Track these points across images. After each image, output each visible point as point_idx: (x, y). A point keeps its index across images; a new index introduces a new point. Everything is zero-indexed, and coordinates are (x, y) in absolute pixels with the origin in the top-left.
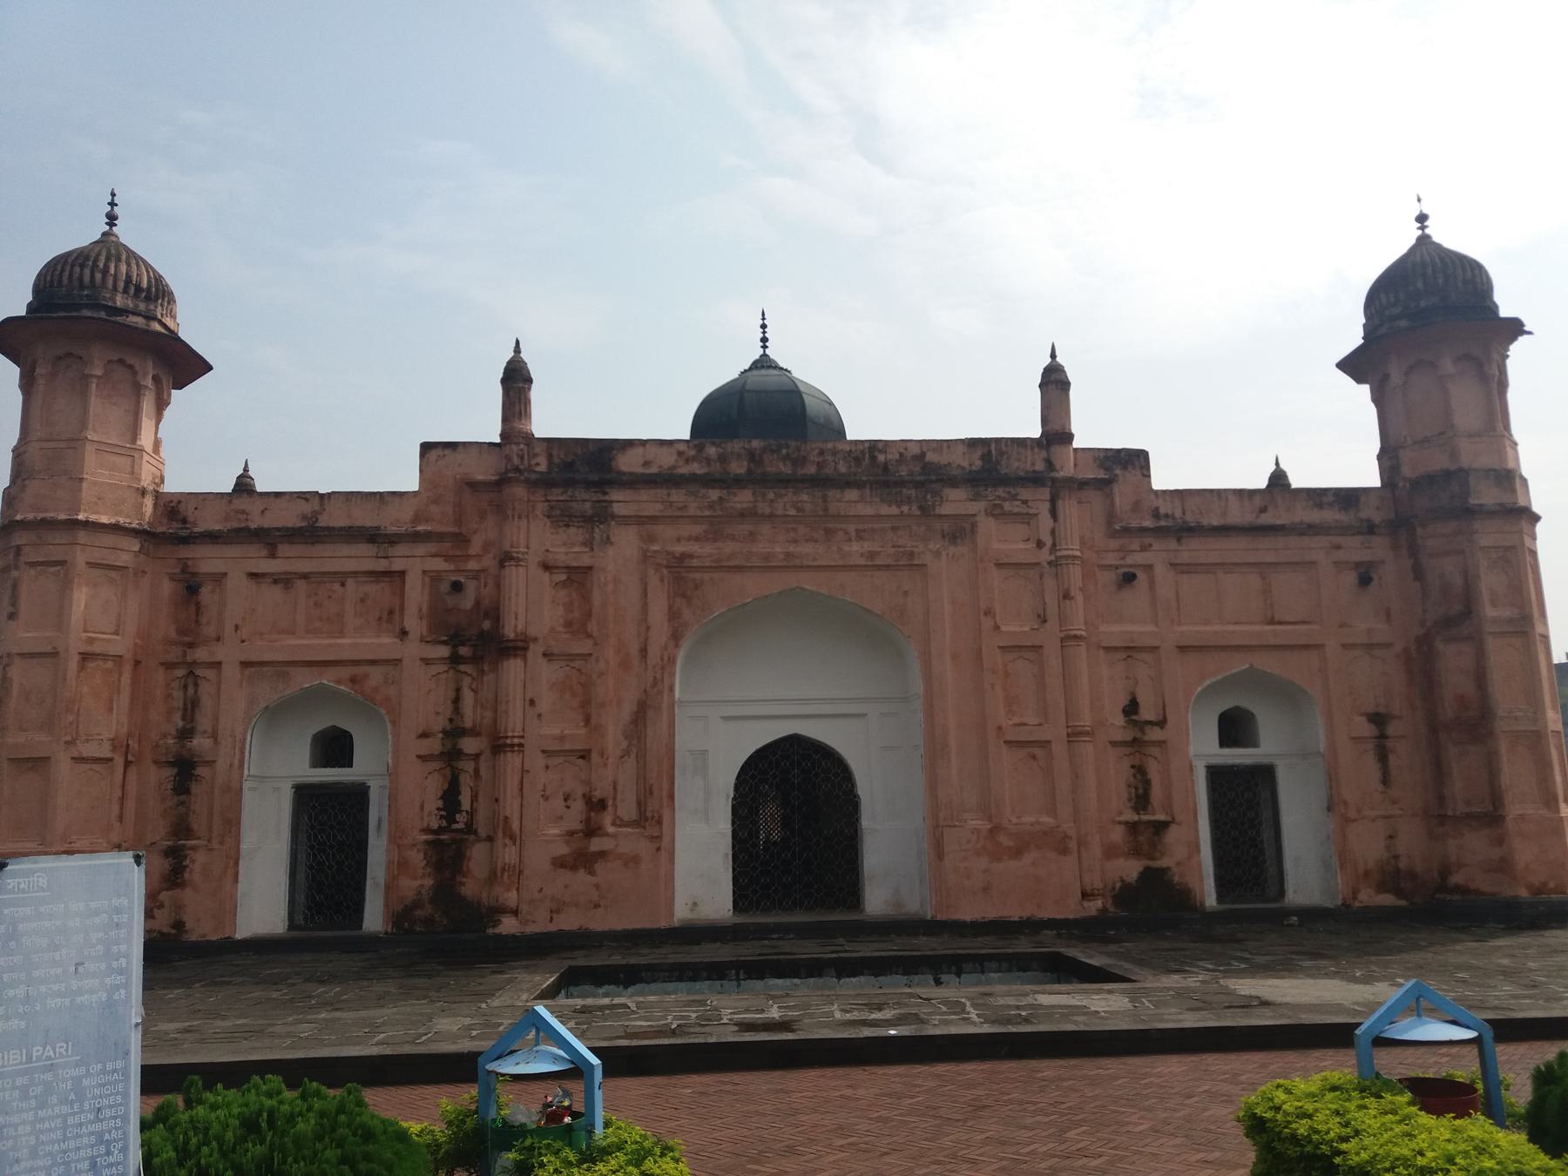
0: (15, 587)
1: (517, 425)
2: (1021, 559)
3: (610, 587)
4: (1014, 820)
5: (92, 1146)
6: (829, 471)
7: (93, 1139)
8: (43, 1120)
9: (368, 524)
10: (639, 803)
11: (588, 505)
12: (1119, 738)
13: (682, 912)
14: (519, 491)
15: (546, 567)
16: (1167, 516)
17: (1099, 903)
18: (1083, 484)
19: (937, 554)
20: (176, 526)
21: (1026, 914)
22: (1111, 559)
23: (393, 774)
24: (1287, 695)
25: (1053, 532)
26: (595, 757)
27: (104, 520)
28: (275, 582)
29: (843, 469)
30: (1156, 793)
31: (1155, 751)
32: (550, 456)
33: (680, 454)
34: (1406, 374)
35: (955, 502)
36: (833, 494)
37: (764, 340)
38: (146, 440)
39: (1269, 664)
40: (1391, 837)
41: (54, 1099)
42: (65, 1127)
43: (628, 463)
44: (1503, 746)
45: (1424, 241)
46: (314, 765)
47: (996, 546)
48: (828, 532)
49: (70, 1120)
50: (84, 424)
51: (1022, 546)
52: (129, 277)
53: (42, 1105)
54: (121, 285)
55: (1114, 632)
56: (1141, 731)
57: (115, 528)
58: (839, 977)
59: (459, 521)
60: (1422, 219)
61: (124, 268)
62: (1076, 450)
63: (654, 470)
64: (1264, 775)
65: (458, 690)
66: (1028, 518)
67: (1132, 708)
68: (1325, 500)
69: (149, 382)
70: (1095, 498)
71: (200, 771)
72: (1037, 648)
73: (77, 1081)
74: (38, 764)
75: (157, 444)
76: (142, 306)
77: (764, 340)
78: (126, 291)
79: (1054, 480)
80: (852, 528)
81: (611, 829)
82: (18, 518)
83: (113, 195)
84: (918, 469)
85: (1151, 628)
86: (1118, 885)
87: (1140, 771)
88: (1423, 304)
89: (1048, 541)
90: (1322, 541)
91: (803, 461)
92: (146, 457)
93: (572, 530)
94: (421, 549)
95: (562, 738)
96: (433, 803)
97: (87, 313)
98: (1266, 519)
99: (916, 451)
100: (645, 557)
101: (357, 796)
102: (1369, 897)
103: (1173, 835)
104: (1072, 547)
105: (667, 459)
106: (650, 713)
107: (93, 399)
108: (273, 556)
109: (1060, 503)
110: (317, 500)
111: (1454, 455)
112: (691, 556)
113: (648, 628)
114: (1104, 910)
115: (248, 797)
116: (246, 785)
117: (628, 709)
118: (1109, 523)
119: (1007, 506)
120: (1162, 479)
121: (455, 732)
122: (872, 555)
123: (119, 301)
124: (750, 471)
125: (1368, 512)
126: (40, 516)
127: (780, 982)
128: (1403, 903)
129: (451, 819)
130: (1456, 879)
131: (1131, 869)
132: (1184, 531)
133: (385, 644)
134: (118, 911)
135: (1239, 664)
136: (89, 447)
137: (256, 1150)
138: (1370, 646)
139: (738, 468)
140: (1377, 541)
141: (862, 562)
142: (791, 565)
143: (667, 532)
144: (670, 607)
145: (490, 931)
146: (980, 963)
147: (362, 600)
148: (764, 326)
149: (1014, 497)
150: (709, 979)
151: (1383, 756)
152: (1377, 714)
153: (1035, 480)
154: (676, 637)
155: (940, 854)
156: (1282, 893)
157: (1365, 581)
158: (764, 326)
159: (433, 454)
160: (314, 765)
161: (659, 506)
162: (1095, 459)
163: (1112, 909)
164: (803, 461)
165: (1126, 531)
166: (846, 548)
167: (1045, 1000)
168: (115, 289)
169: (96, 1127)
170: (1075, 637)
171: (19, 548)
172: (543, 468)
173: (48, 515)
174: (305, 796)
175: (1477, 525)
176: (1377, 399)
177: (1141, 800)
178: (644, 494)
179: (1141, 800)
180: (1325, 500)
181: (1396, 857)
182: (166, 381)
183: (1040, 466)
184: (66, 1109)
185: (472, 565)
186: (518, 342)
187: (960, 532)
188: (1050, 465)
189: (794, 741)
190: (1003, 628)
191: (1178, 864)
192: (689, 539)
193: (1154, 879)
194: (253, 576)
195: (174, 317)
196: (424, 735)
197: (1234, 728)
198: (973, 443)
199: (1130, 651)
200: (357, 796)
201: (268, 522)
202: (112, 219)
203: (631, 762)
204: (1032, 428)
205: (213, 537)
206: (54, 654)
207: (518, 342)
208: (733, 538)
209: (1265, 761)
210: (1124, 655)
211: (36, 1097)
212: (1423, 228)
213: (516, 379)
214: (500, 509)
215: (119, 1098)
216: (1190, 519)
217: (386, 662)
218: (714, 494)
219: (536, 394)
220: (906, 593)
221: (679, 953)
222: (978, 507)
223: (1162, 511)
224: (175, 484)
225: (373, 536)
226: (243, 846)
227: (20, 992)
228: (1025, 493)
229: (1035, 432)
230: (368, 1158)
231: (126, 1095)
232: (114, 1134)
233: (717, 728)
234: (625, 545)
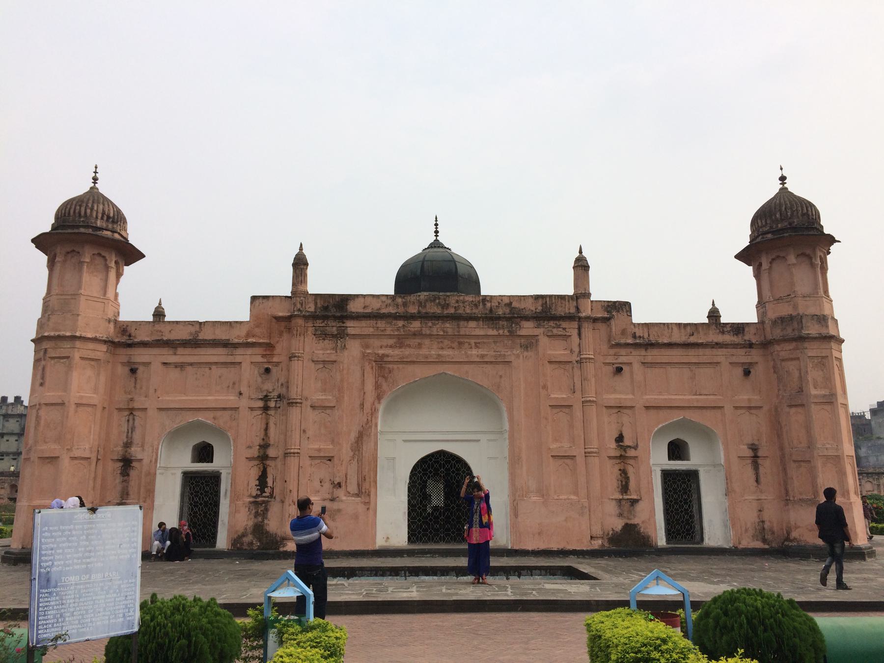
0: (44, 369)
1: (301, 288)
3: (345, 372)
4: (556, 497)
6: (460, 311)
9: (224, 338)
10: (358, 485)
11: (335, 328)
12: (613, 454)
13: (380, 543)
14: (300, 322)
16: (640, 337)
17: (600, 542)
18: (595, 320)
19: (518, 356)
20: (125, 339)
21: (561, 547)
22: (610, 359)
23: (234, 467)
24: (706, 434)
25: (579, 345)
26: (336, 460)
27: (89, 336)
28: (176, 367)
29: (468, 311)
30: (632, 484)
31: (631, 462)
32: (316, 304)
34: (771, 263)
35: (528, 328)
36: (462, 323)
37: (437, 232)
38: (110, 295)
39: (694, 417)
40: (760, 511)
44: (819, 463)
45: (784, 190)
46: (193, 461)
47: (549, 352)
48: (460, 343)
50: (80, 288)
52: (103, 210)
54: (100, 215)
55: (612, 398)
56: (624, 452)
57: (95, 340)
58: (457, 576)
60: (783, 179)
61: (101, 207)
63: (369, 310)
64: (692, 476)
65: (267, 424)
66: (566, 337)
67: (620, 439)
68: (725, 329)
69: (113, 264)
70: (601, 326)
71: (134, 464)
72: (570, 406)
73: (119, 586)
74: (53, 460)
75: (116, 295)
76: (110, 226)
77: (437, 232)
78: (102, 218)
79: (580, 318)
81: (344, 498)
82: (46, 334)
83: (96, 167)
84: (508, 311)
85: (631, 396)
86: (611, 533)
87: (624, 472)
88: (779, 226)
89: (576, 350)
90: (724, 351)
91: (447, 306)
92: (111, 303)
93: (326, 342)
94: (250, 351)
95: (319, 450)
96: (254, 482)
97: (82, 230)
98: (692, 340)
99: (507, 301)
100: (364, 356)
101: (214, 478)
102: (748, 542)
103: (639, 507)
104: (589, 354)
105: (375, 305)
106: (365, 438)
107: (85, 274)
108: (175, 354)
109: (583, 330)
110: (198, 326)
111: (795, 307)
112: (388, 356)
114: (603, 545)
115: (159, 478)
116: (158, 472)
117: (353, 435)
118: (609, 341)
119: (555, 331)
120: (639, 316)
121: (264, 446)
122: (483, 356)
123: (99, 223)
124: (419, 312)
125: (750, 336)
126: (57, 333)
127: (427, 578)
128: (767, 547)
129: (262, 490)
130: (794, 534)
131: (618, 525)
132: (650, 345)
133: (231, 399)
134: (134, 526)
135: (677, 416)
136: (82, 298)
137: (178, 617)
138: (750, 408)
139: (413, 310)
140: (754, 351)
142: (440, 361)
144: (376, 382)
145: (281, 549)
146: (531, 571)
147: (220, 377)
148: (436, 225)
149: (558, 327)
150: (390, 575)
151: (756, 466)
152: (753, 444)
153: (570, 318)
154: (379, 398)
155: (516, 515)
156: (702, 539)
157: (747, 373)
158: (436, 225)
159: (257, 302)
160: (193, 461)
161: (371, 330)
162: (602, 307)
163: (606, 545)
164: (447, 306)
165: (618, 345)
167: (547, 586)
168: (97, 218)
169: (125, 602)
170: (590, 401)
171: (46, 350)
172: (312, 309)
173: (61, 333)
174: (189, 478)
175: (806, 345)
176: (757, 275)
177: (625, 488)
178: (364, 323)
179: (625, 488)
180: (725, 329)
181: (763, 522)
182: (121, 263)
183: (573, 310)
185: (275, 359)
187: (530, 343)
188: (577, 308)
189: (442, 453)
191: (643, 522)
192: (387, 346)
193: (630, 529)
194: (165, 364)
195: (126, 230)
196: (249, 447)
197: (677, 450)
198: (537, 297)
199: (620, 408)
200: (214, 478)
201: (173, 336)
202: (95, 179)
203: (355, 462)
204: (570, 291)
205: (144, 344)
206: (63, 404)
208: (409, 346)
209: (694, 468)
210: (617, 410)
212: (783, 184)
213: (300, 264)
214: (289, 330)
216: (653, 339)
217: (231, 409)
218: (400, 323)
219: (310, 271)
220: (501, 377)
221: (380, 563)
222: (539, 331)
223: (637, 335)
224: (125, 316)
225: (226, 344)
226: (156, 503)
227: (102, 553)
228: (564, 324)
229: (570, 291)
230: (217, 622)
231: (135, 592)
233: (402, 444)
234: (354, 348)
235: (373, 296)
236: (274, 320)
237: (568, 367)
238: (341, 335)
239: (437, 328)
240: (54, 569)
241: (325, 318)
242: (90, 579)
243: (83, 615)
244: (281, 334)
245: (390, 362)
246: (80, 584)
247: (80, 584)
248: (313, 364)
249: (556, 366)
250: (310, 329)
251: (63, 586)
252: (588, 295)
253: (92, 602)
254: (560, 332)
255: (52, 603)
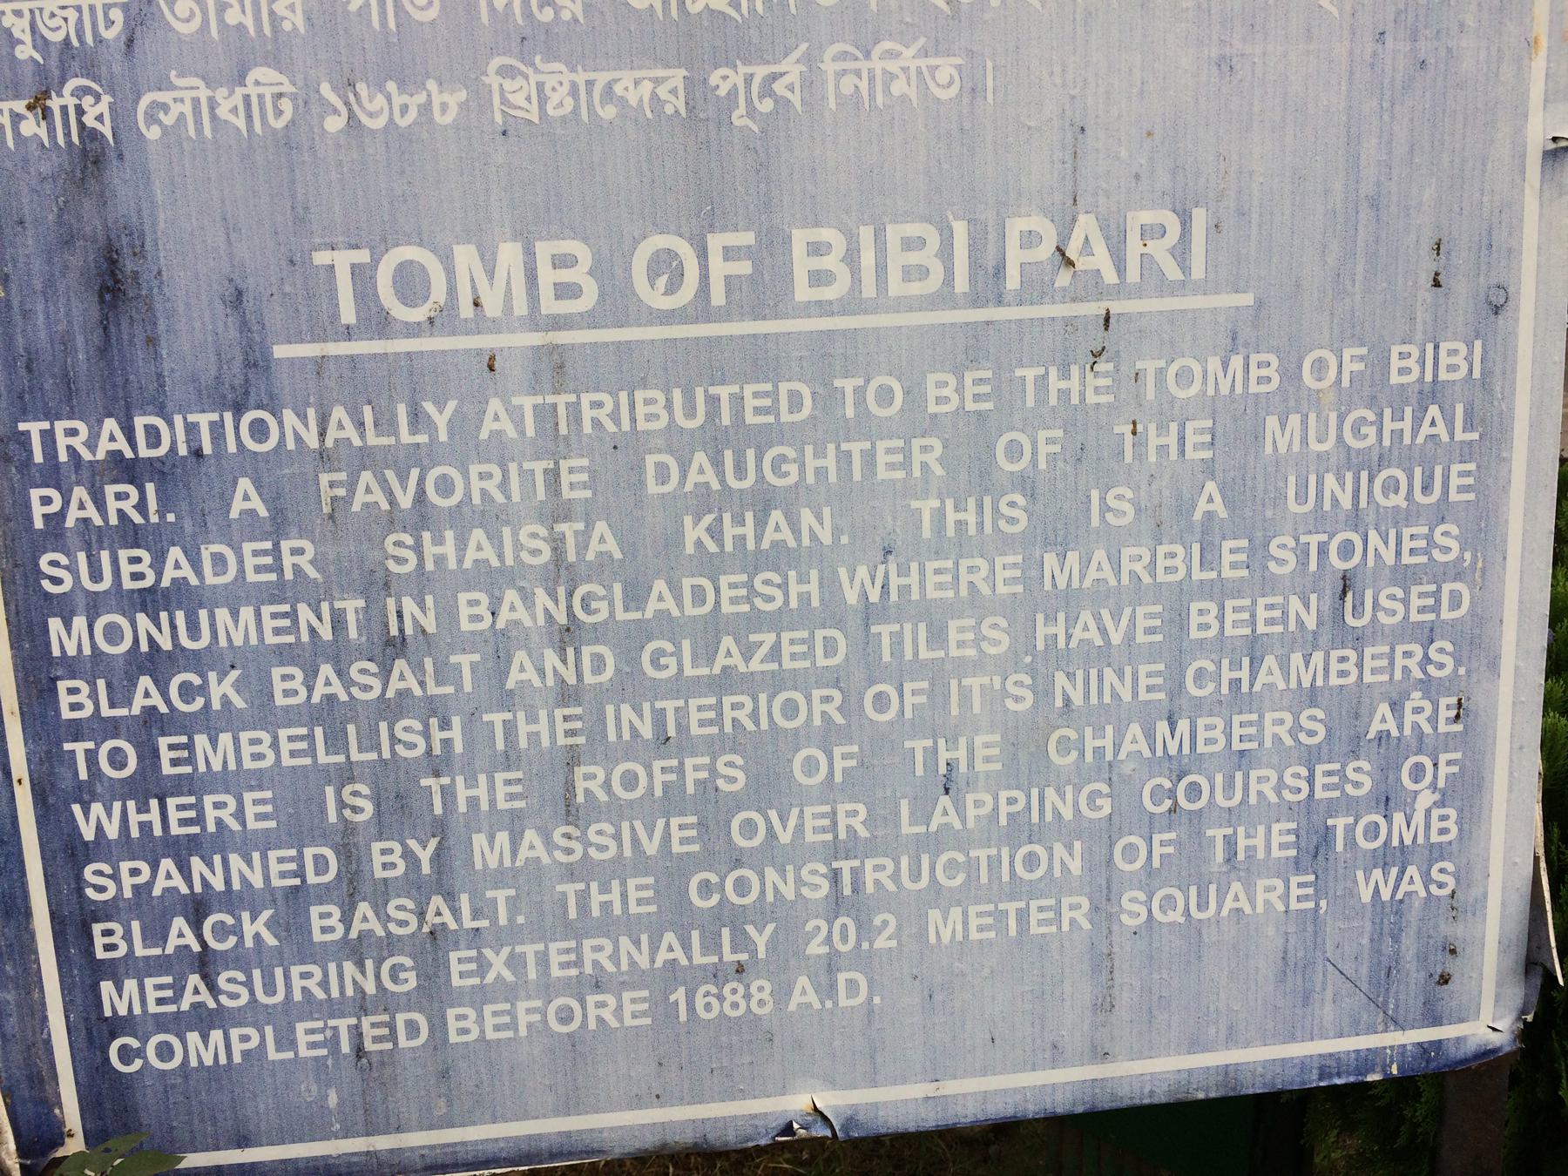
5: (1311, 758)
7: (1314, 722)
8: (1069, 602)
41: (1122, 504)
42: (1176, 649)
49: (1202, 618)
53: (1059, 531)
169: (1337, 669)
184: (1177, 561)
211: (1025, 483)
215: (1449, 538)
232: (1417, 714)
240: (176, 106)
242: (764, 290)
243: (711, 809)
246: (627, 369)
247: (627, 369)
251: (361, 385)
253: (833, 649)
255: (236, 628)
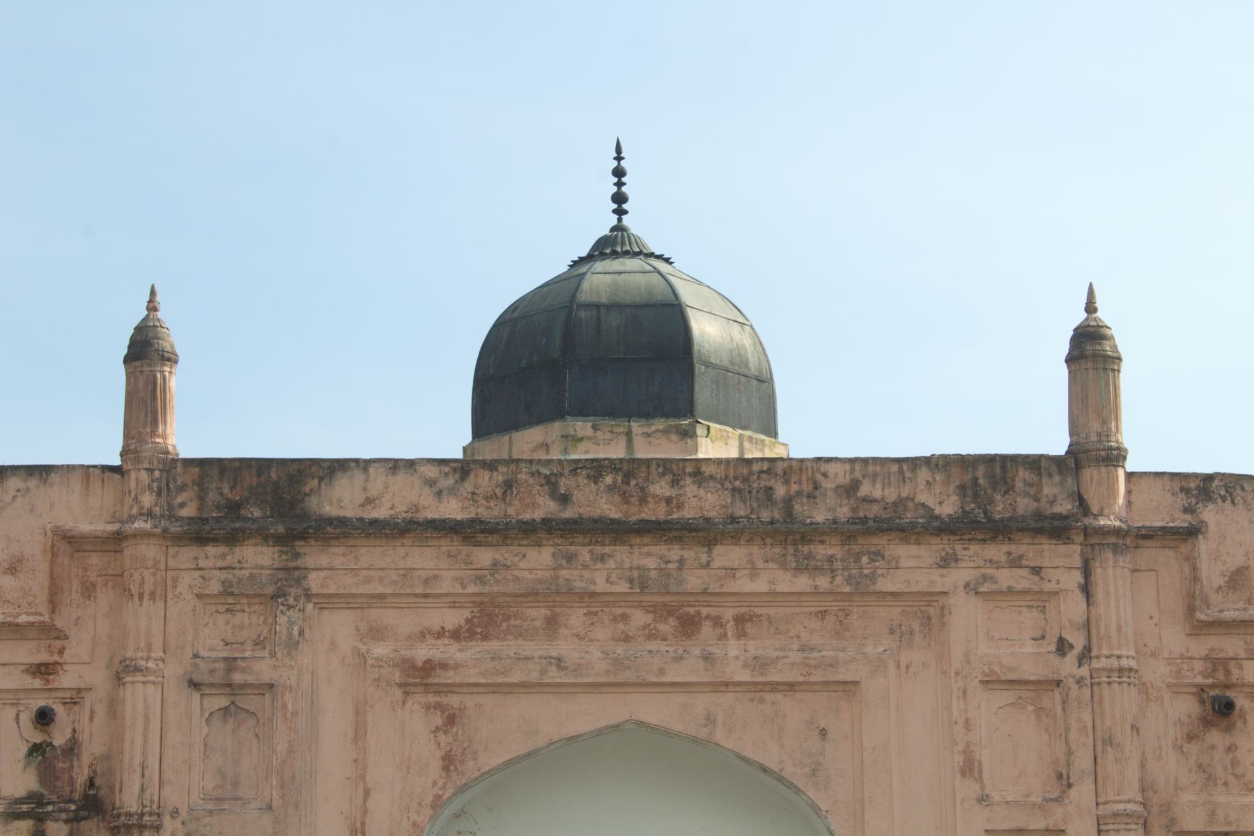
2: (1030, 671)
14: (150, 551)
15: (194, 685)
33: (431, 483)
35: (912, 567)
37: (620, 198)
43: (340, 500)
51: (1030, 648)
59: (54, 606)
62: (1130, 476)
63: (382, 513)
66: (1041, 599)
70: (1166, 560)
77: (620, 198)
79: (1086, 532)
80: (729, 614)
89: (1078, 641)
93: (239, 618)
99: (844, 479)
109: (1097, 572)
112: (444, 666)
113: (367, 793)
118: (1191, 610)
119: (1007, 578)
122: (759, 664)
141: (745, 676)
143: (404, 622)
148: (619, 173)
153: (1055, 528)
158: (619, 173)
166: (717, 651)
170: (1116, 815)
186: (153, 287)
190: (996, 797)
192: (441, 634)
207: (153, 287)
213: (146, 352)
214: (118, 580)
218: (484, 556)
219: (180, 383)
229: (1056, 442)
235: (393, 465)
236: (63, 547)
237: (1053, 701)
238: (285, 589)
239: (605, 571)
241: (233, 539)
244: (88, 590)
245: (452, 688)
248: (196, 697)
249: (1008, 696)
250: (187, 580)
252: (1115, 456)
254: (1018, 579)
